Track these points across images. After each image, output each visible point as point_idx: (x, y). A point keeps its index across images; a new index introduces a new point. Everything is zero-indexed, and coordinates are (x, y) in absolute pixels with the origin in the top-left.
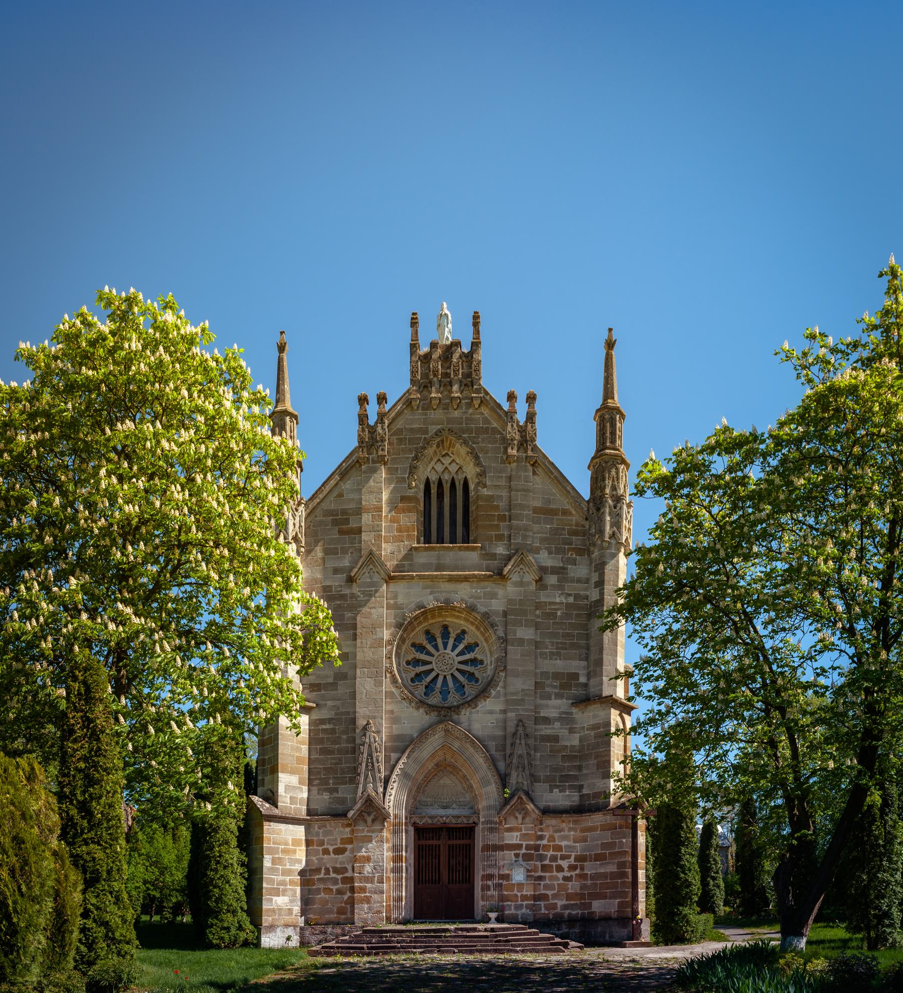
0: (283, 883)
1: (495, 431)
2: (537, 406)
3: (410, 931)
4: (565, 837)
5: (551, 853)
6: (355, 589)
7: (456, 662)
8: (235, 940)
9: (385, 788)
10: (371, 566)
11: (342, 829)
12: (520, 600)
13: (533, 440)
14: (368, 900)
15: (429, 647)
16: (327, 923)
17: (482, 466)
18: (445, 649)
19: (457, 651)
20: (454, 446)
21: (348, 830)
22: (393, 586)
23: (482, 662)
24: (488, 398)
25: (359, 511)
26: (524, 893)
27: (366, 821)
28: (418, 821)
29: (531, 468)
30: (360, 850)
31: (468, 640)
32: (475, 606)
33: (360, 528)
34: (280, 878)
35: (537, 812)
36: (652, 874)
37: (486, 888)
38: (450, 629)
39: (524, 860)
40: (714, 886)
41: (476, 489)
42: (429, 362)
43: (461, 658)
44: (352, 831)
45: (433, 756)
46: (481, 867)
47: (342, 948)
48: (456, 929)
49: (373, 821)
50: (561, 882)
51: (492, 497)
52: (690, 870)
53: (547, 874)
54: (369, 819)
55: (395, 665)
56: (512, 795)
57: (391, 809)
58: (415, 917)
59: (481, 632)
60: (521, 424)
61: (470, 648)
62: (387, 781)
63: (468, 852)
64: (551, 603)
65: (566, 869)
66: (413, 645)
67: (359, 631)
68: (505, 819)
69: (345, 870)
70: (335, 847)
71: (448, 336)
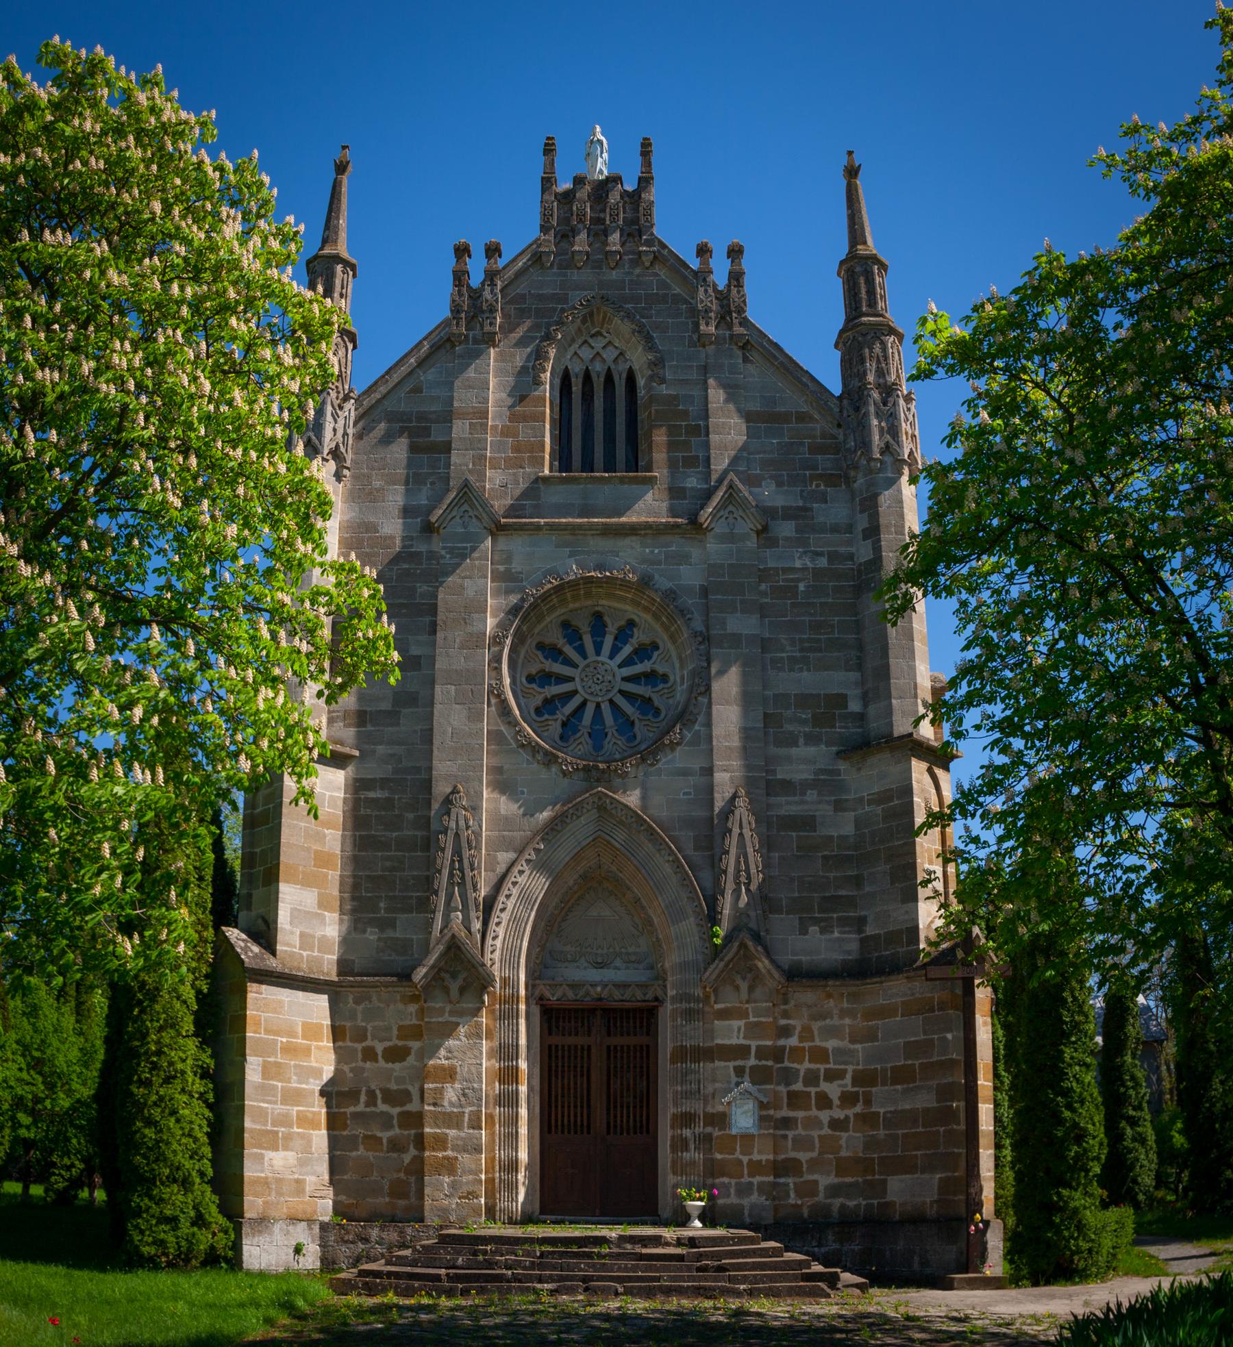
0: (284, 1120)
1: (677, 299)
2: (746, 263)
3: (531, 1241)
4: (833, 1032)
5: (807, 1065)
6: (437, 545)
7: (618, 678)
8: (190, 1250)
9: (485, 923)
10: (466, 507)
11: (401, 1006)
12: (731, 565)
13: (741, 310)
14: (449, 1166)
15: (569, 651)
16: (370, 1219)
17: (658, 351)
18: (598, 653)
19: (620, 658)
20: (610, 321)
21: (413, 1008)
22: (503, 543)
23: (665, 678)
24: (665, 252)
25: (447, 417)
26: (756, 1157)
27: (447, 991)
28: (548, 994)
29: (739, 353)
30: (433, 1052)
31: (639, 637)
32: (651, 578)
33: (450, 443)
34: (280, 1108)
35: (776, 975)
36: (1007, 1113)
37: (680, 1144)
38: (606, 618)
39: (753, 1083)
40: (1134, 1140)
41: (648, 387)
42: (571, 203)
43: (627, 671)
44: (421, 1012)
45: (577, 858)
46: (670, 1096)
47: (397, 1275)
48: (622, 1239)
49: (462, 990)
50: (826, 1131)
51: (675, 397)
52: (1082, 1102)
53: (800, 1114)
54: (454, 987)
55: (507, 681)
56: (728, 939)
57: (497, 966)
58: (543, 1211)
59: (663, 624)
60: (720, 288)
61: (643, 652)
62: (488, 907)
63: (646, 1058)
64: (785, 570)
65: (836, 1102)
66: (540, 646)
67: (441, 616)
68: (715, 991)
69: (405, 1097)
70: (388, 1044)
71: (602, 167)
